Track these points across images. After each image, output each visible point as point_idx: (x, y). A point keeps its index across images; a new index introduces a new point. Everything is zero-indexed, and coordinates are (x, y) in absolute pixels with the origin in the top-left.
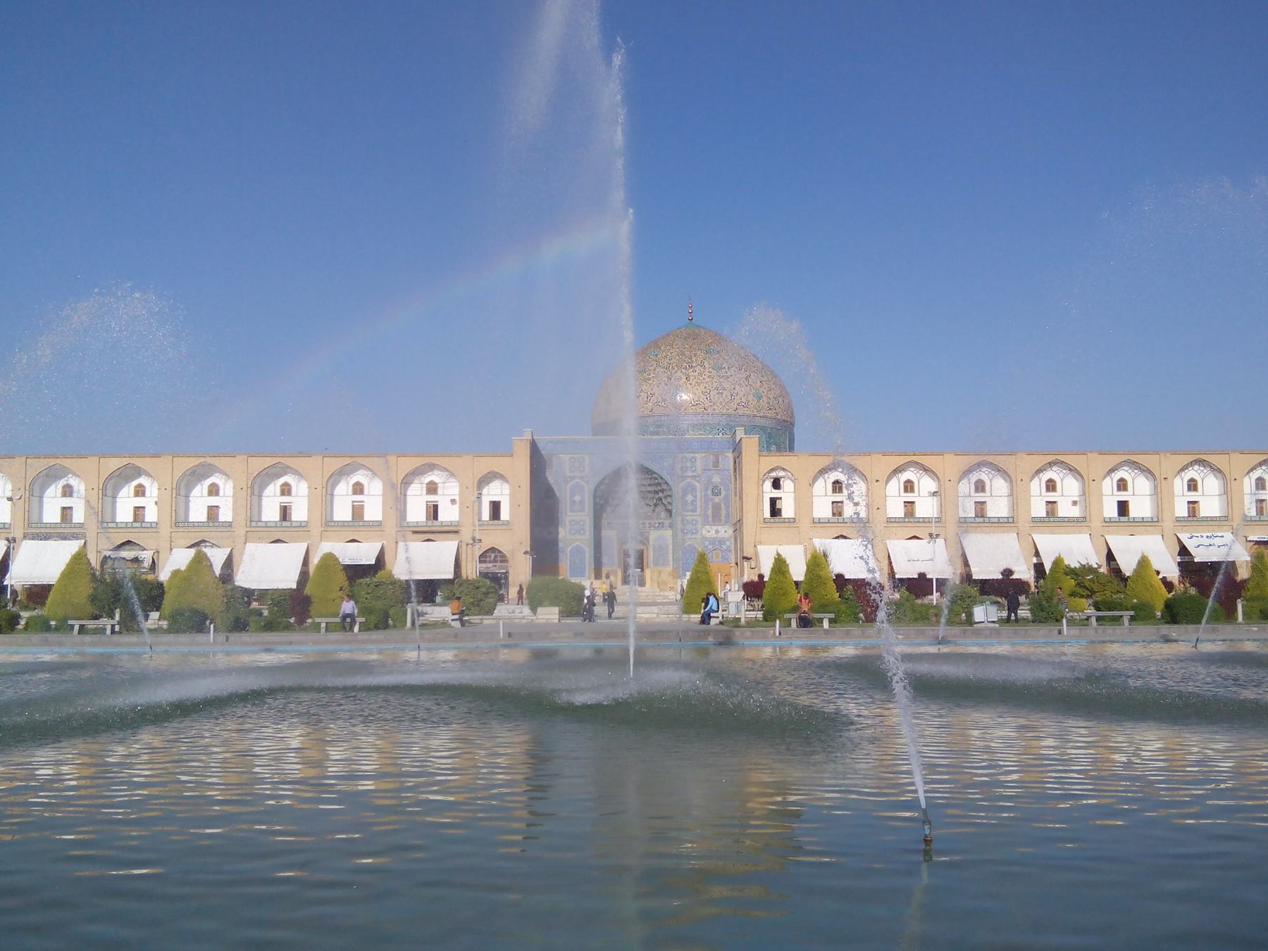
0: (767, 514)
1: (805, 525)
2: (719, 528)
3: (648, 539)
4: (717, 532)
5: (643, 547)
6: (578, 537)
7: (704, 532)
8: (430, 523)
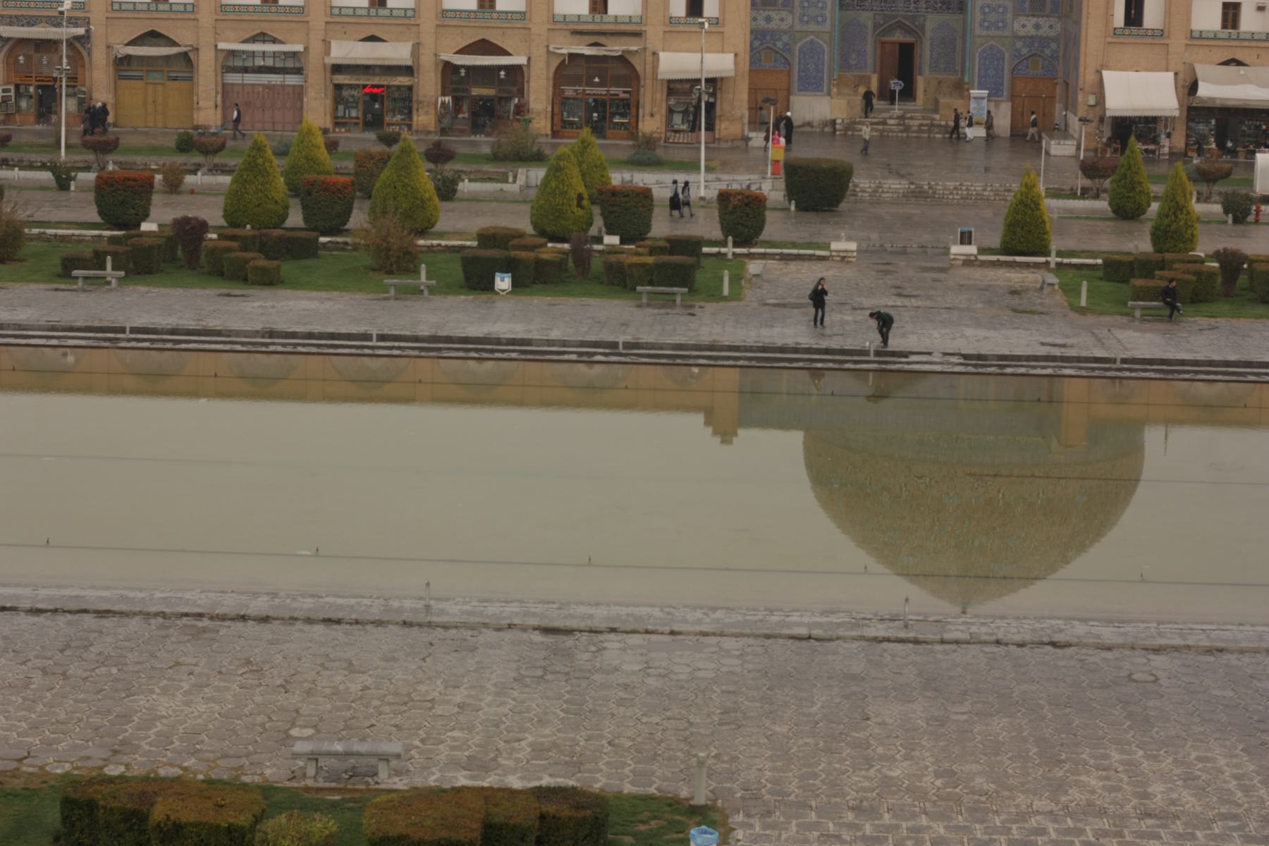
0: (1119, 18)
1: (1177, 42)
2: (1041, 21)
3: (922, 28)
4: (1037, 26)
5: (908, 39)
6: (813, 27)
7: (1016, 26)
8: (598, 17)
